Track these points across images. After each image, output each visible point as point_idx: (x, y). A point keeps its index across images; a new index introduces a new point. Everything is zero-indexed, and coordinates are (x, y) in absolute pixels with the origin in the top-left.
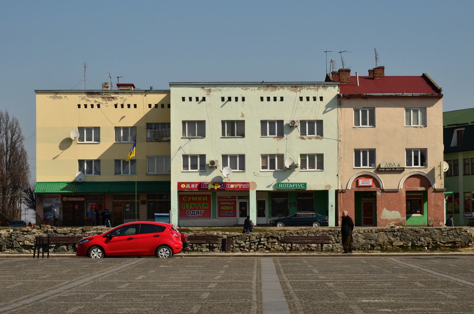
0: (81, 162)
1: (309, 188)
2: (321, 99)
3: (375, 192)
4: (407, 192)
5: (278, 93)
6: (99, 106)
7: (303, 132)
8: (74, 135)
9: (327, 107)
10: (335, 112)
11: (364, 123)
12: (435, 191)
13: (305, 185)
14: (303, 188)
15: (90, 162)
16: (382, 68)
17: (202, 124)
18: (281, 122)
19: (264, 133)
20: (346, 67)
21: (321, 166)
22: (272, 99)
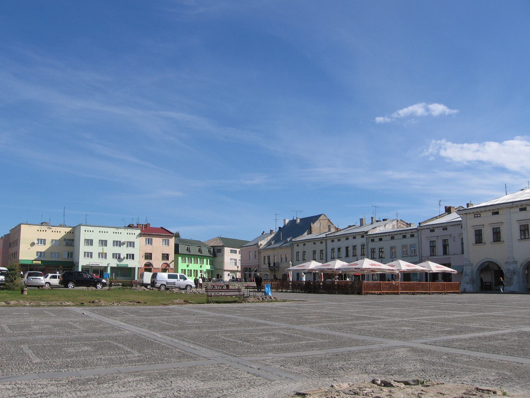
0: (37, 252)
1: (129, 266)
2: (134, 234)
3: (151, 269)
4: (162, 269)
5: (120, 230)
6: (46, 231)
7: (127, 246)
8: (36, 242)
9: (137, 236)
10: (139, 239)
11: (149, 243)
12: (171, 269)
13: (128, 265)
15: (41, 253)
17: (106, 241)
18: (120, 242)
19: (114, 245)
21: (133, 258)
22: (117, 233)
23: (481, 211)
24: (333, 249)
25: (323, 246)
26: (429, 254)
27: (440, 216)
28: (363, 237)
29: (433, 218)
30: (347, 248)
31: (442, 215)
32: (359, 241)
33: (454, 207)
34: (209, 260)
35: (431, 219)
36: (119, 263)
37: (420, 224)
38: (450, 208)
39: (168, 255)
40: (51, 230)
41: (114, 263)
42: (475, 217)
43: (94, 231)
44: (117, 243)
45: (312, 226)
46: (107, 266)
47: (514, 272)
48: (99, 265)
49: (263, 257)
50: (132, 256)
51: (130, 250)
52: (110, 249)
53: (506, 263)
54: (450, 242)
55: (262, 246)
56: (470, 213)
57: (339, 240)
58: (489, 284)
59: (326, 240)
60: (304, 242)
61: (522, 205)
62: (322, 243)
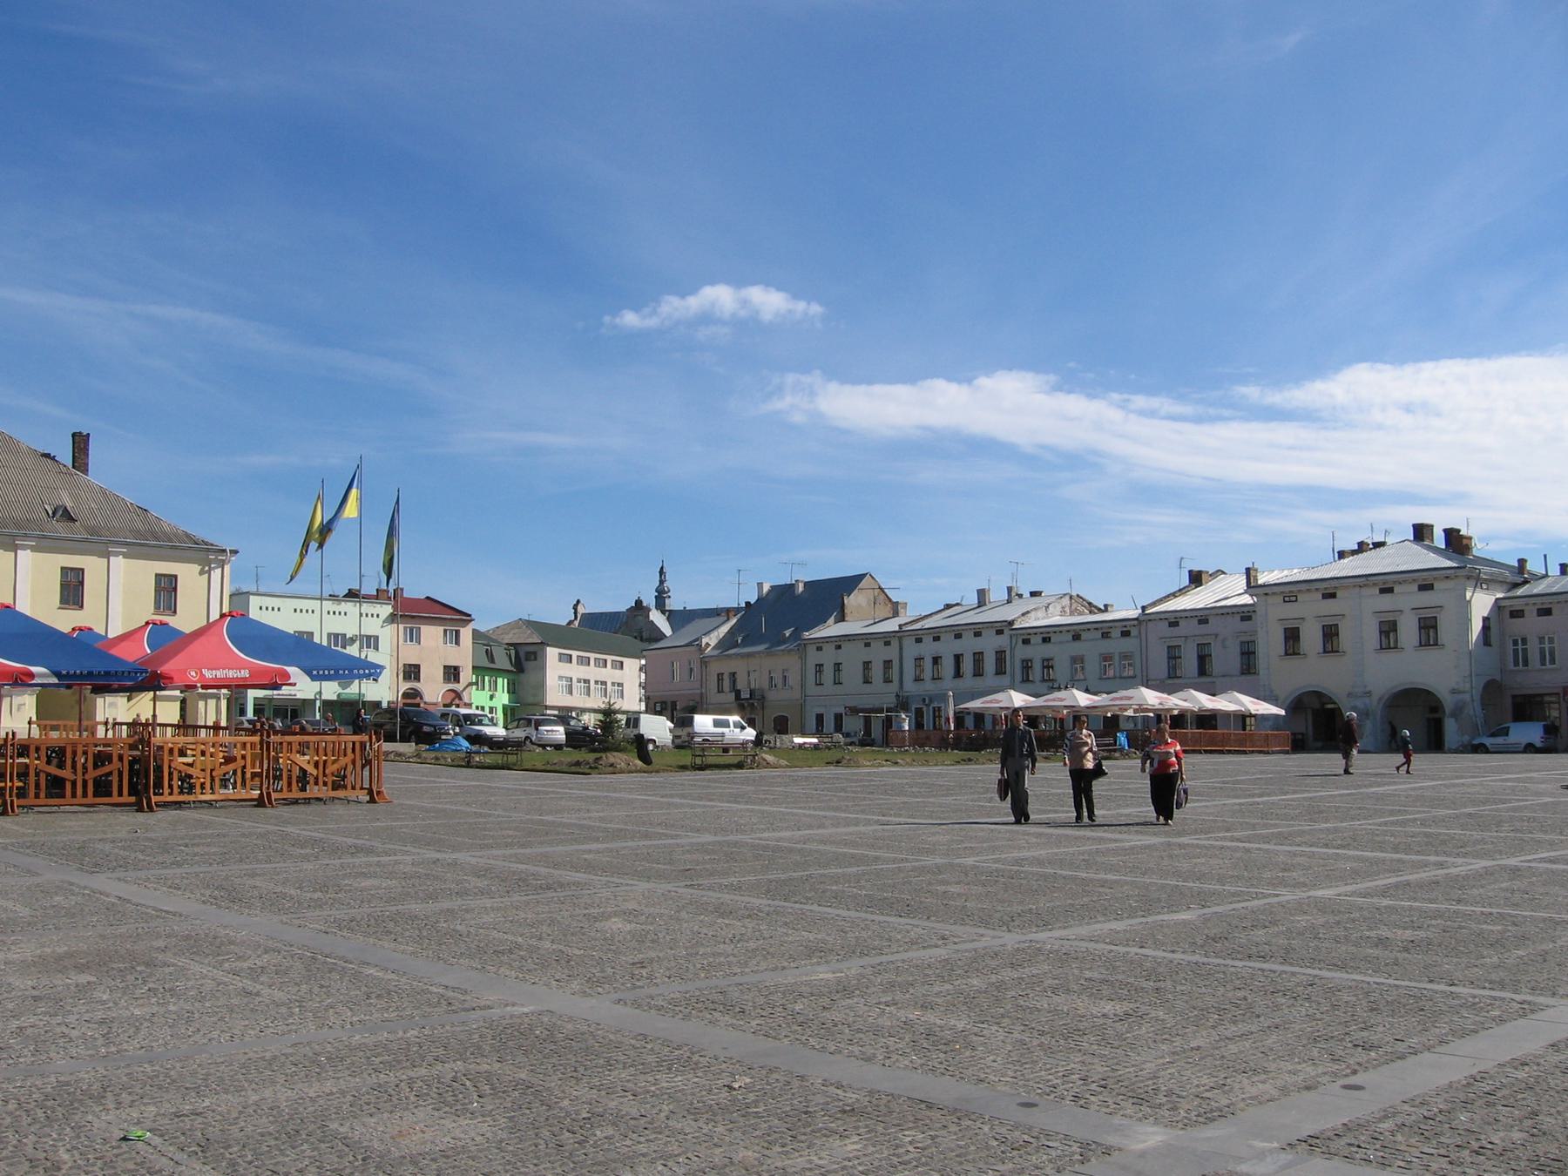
2: (378, 616)
9: (384, 622)
11: (411, 640)
18: (345, 635)
22: (337, 613)
23: (1299, 591)
24: (919, 659)
25: (892, 653)
26: (1166, 675)
27: (1182, 591)
28: (1000, 632)
29: (1168, 596)
31: (1184, 588)
32: (989, 644)
33: (1208, 572)
34: (506, 680)
35: (1165, 597)
36: (341, 691)
37: (1144, 608)
38: (1200, 573)
39: (456, 669)
42: (1285, 601)
43: (281, 609)
45: (846, 602)
46: (313, 698)
47: (1365, 714)
48: (295, 695)
49: (716, 676)
53: (1349, 695)
54: (1215, 651)
55: (711, 647)
56: (1274, 594)
57: (937, 639)
58: (1300, 737)
59: (900, 638)
60: (839, 642)
61: (1384, 583)
62: (887, 644)
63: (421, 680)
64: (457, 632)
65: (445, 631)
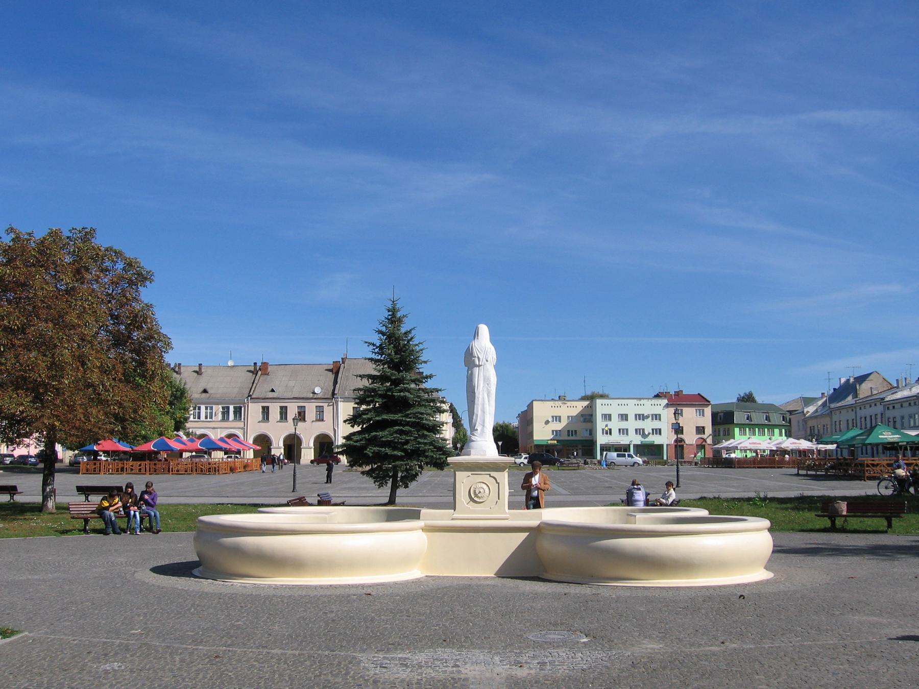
0: (553, 431)
1: (655, 443)
2: (660, 405)
3: (683, 445)
4: (697, 445)
5: (642, 402)
6: (560, 407)
7: (652, 419)
8: (550, 420)
9: (664, 407)
10: (666, 410)
12: (709, 444)
13: (654, 442)
14: (652, 443)
15: (556, 431)
16: (682, 391)
18: (643, 415)
19: (636, 419)
20: (668, 391)
21: (660, 434)
30: (871, 416)
34: (783, 430)
36: (643, 440)
39: (703, 428)
40: (566, 406)
41: (638, 440)
44: (641, 417)
45: (858, 388)
46: (629, 443)
50: (658, 431)
51: (656, 424)
52: (632, 424)
59: (855, 407)
63: (684, 434)
64: (703, 410)
65: (696, 410)
